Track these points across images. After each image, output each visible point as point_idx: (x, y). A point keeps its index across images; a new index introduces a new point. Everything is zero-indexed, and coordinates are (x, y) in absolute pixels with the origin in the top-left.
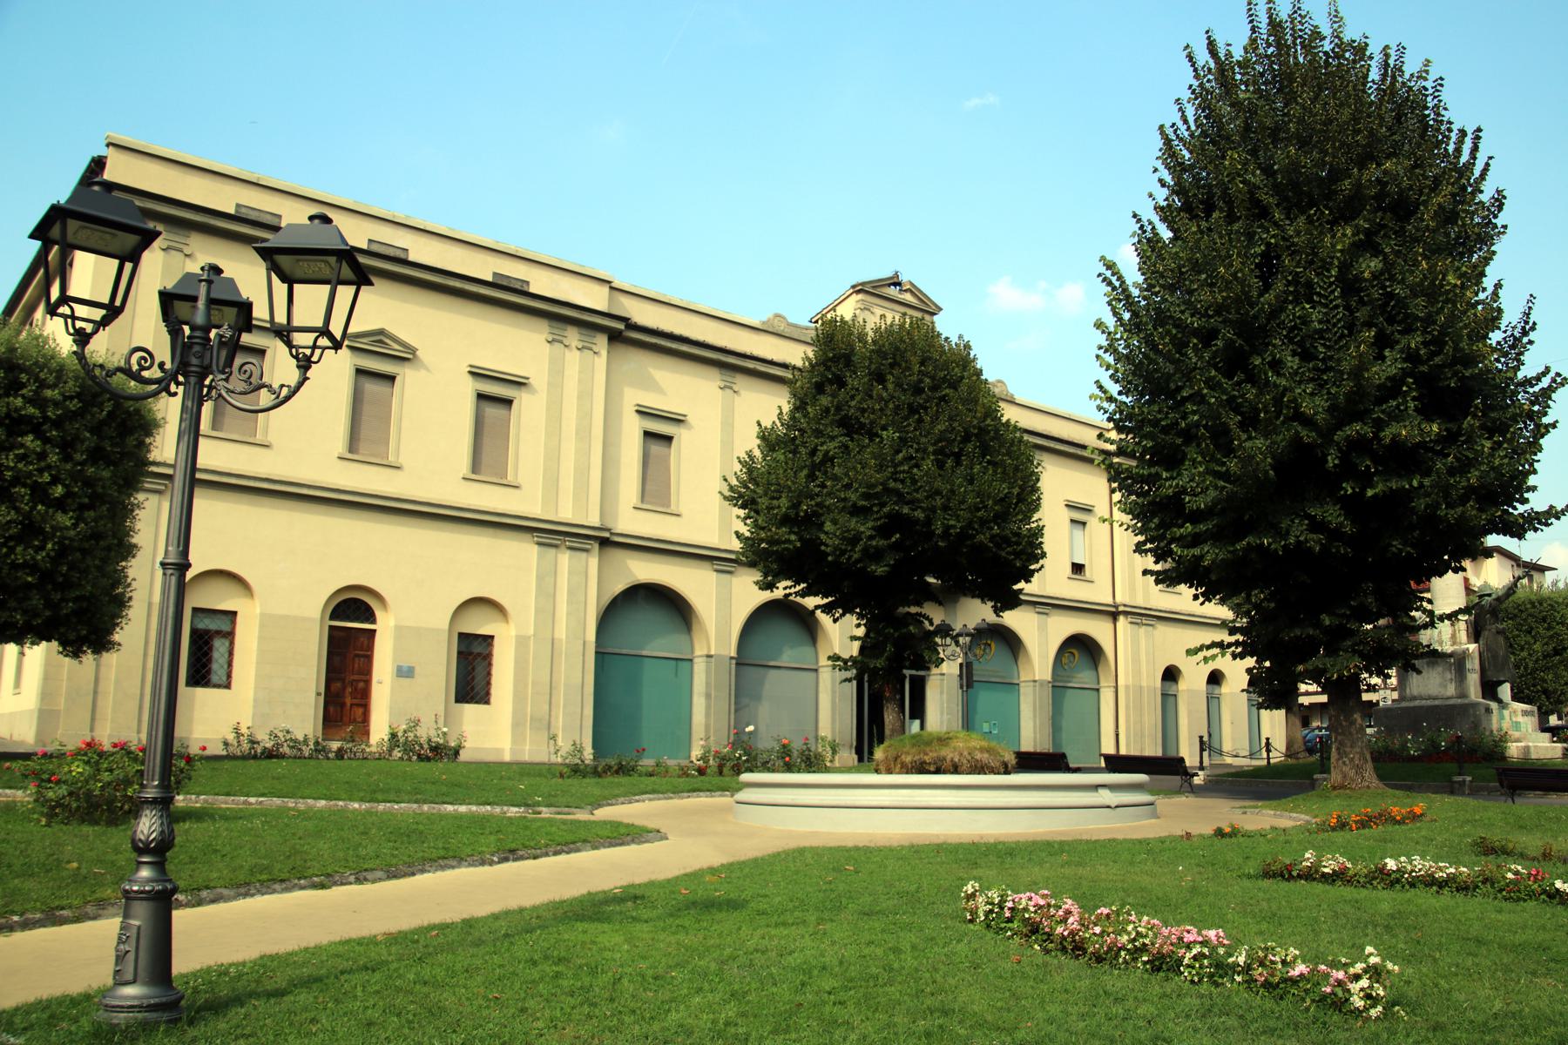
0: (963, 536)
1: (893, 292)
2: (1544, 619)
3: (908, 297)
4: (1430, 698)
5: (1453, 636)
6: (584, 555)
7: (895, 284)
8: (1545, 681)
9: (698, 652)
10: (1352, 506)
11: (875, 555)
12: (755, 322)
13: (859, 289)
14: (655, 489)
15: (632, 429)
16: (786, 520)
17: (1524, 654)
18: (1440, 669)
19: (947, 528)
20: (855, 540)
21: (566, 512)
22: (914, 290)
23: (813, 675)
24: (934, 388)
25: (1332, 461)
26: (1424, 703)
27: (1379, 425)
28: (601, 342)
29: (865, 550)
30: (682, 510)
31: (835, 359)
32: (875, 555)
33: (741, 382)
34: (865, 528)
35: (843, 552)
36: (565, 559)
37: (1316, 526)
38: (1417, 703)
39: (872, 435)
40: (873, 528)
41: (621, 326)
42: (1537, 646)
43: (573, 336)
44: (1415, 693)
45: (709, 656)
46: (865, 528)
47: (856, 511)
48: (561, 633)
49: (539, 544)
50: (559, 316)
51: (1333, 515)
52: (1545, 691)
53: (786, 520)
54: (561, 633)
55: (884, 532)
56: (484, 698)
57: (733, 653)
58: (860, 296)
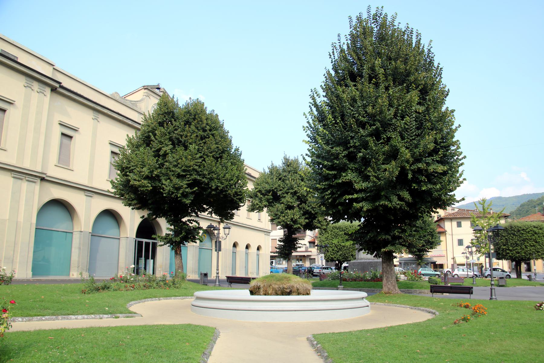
1: (157, 91)
6: (34, 184)
7: (159, 88)
9: (75, 230)
10: (412, 193)
11: (185, 195)
12: (108, 94)
13: (146, 88)
14: (64, 159)
15: (58, 130)
16: (147, 178)
19: (217, 187)
20: (178, 189)
21: (27, 164)
24: (210, 130)
25: (410, 176)
26: (366, 261)
27: (428, 164)
28: (48, 90)
29: (182, 194)
30: (74, 168)
31: (168, 113)
32: (185, 195)
33: (101, 118)
34: (184, 183)
35: (173, 193)
36: (25, 185)
37: (401, 199)
38: (363, 261)
39: (186, 148)
40: (187, 184)
41: (57, 85)
43: (36, 86)
45: (81, 232)
46: (184, 183)
47: (179, 176)
48: (21, 218)
49: (14, 177)
50: (31, 75)
51: (406, 195)
53: (147, 178)
54: (21, 218)
55: (190, 186)
57: (90, 231)
58: (146, 91)
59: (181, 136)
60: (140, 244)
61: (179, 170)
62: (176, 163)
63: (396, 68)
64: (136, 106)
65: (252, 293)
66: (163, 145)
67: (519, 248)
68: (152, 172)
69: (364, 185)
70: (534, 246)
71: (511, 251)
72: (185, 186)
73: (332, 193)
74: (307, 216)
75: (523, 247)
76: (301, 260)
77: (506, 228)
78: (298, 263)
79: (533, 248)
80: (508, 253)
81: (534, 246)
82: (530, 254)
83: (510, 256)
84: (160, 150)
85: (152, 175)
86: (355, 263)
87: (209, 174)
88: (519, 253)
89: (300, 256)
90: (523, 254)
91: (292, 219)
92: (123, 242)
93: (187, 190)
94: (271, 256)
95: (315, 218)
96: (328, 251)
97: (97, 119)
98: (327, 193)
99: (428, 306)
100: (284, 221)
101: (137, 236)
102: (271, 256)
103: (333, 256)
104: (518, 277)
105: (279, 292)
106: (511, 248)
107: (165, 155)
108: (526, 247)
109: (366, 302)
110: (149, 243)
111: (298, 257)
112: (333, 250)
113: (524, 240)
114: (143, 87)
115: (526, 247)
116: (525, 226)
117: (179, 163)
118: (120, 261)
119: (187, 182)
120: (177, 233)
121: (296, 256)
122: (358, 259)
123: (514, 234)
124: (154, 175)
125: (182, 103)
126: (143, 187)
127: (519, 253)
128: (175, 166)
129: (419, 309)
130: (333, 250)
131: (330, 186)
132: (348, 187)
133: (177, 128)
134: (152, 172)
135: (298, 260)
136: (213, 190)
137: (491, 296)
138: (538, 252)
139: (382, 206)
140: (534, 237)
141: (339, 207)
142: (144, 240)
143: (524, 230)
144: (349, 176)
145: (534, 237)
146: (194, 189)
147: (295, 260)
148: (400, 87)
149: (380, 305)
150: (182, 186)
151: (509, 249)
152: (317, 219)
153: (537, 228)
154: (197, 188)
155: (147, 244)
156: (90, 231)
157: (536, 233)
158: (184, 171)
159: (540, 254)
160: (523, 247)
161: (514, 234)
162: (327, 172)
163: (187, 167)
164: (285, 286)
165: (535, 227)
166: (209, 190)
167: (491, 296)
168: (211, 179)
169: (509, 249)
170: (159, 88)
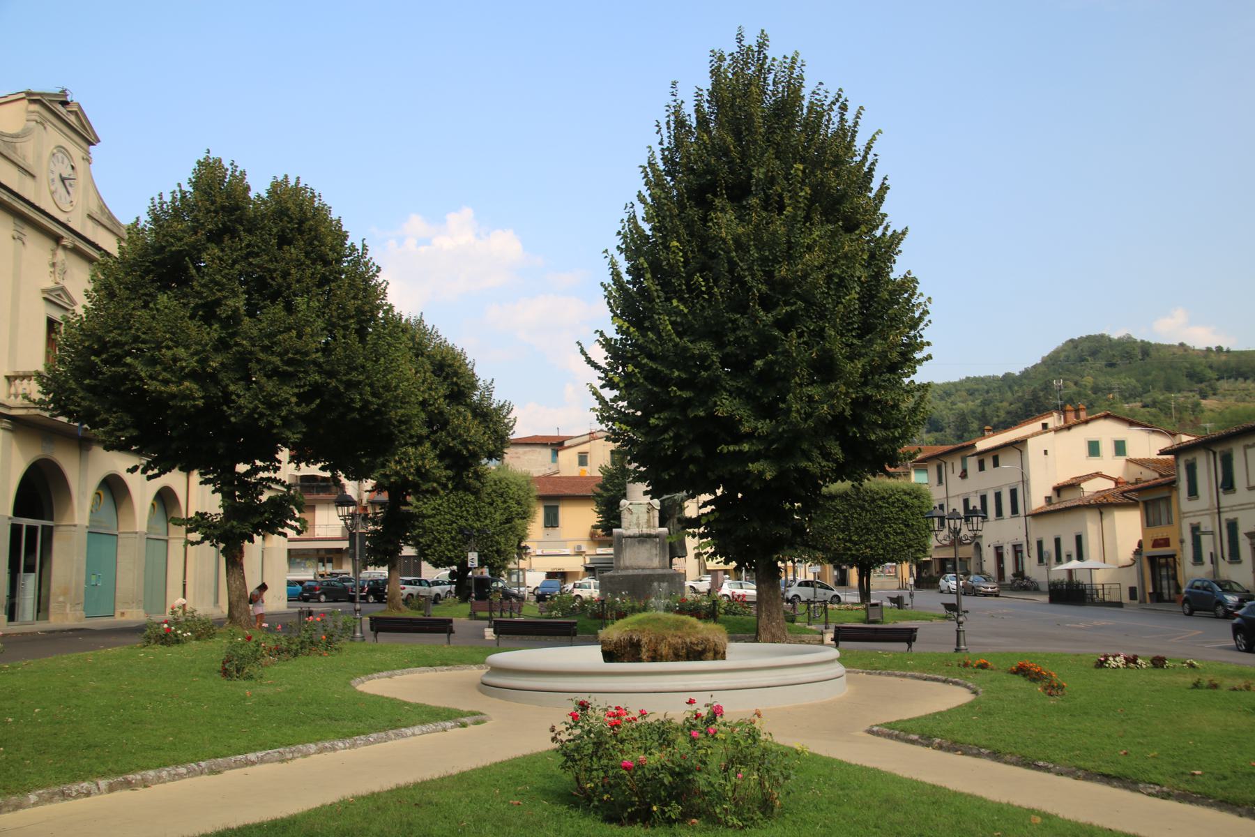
0: (378, 412)
2: (502, 495)
3: (72, 119)
4: (639, 568)
5: (648, 521)
8: (498, 543)
13: (33, 98)
16: (193, 375)
17: (488, 521)
18: (648, 546)
19: (366, 404)
20: (274, 406)
22: (79, 114)
26: (636, 572)
34: (288, 392)
35: (262, 415)
38: (630, 572)
40: (297, 395)
42: (497, 516)
44: (628, 563)
47: (274, 373)
52: (498, 552)
53: (193, 375)
55: (303, 398)
56: (913, 631)
58: (36, 107)
59: (270, 271)
60: (16, 530)
61: (276, 360)
62: (266, 342)
63: (822, 183)
64: (15, 150)
65: (609, 656)
67: (873, 537)
68: (203, 361)
69: (764, 426)
70: (902, 533)
71: (855, 543)
72: (294, 400)
73: (677, 437)
74: (447, 461)
75: (881, 535)
76: (330, 561)
78: (321, 570)
80: (850, 549)
81: (902, 533)
82: (894, 550)
83: (852, 555)
84: (218, 303)
85: (204, 369)
86: (613, 577)
87: (348, 373)
88: (872, 548)
90: (881, 552)
91: (418, 469)
93: (297, 410)
94: (289, 551)
95: (467, 466)
96: (439, 542)
98: (666, 436)
99: (913, 668)
100: (397, 473)
101: (19, 510)
102: (289, 551)
103: (453, 554)
104: (862, 602)
105: (683, 652)
106: (855, 538)
107: (234, 318)
108: (887, 536)
109: (839, 669)
110: (36, 528)
112: (453, 539)
113: (883, 521)
114: (29, 94)
115: (887, 536)
116: (886, 491)
117: (275, 343)
119: (296, 390)
120: (231, 510)
121: (318, 550)
122: (618, 568)
123: (862, 508)
124: (209, 370)
125: (259, 187)
128: (265, 349)
129: (889, 675)
130: (453, 539)
131: (671, 423)
132: (729, 429)
134: (203, 361)
136: (354, 409)
137: (958, 644)
138: (910, 546)
139: (797, 469)
140: (903, 516)
141: (691, 467)
142: (26, 522)
143: (883, 498)
144: (725, 405)
146: (313, 406)
148: (830, 227)
149: (872, 668)
150: (287, 399)
151: (850, 541)
153: (909, 494)
155: (32, 531)
157: (907, 506)
158: (290, 362)
160: (881, 535)
161: (862, 508)
162: (679, 393)
163: (298, 352)
164: (694, 640)
165: (906, 493)
167: (958, 644)
168: (350, 385)
169: (850, 541)
170: (65, 103)
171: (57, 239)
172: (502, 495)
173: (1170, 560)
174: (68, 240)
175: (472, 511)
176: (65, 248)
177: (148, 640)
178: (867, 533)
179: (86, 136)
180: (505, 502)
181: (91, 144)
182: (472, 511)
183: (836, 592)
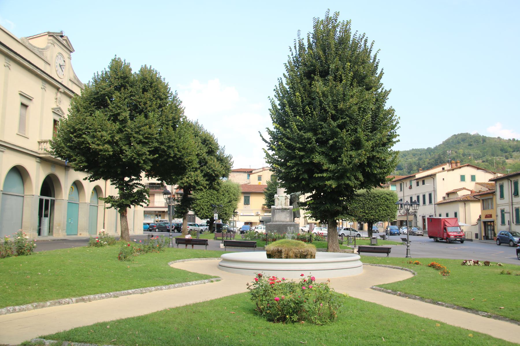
0: (180, 158)
2: (228, 192)
3: (64, 42)
5: (285, 203)
7: (62, 36)
8: (226, 210)
13: (50, 34)
16: (109, 142)
17: (222, 202)
18: (285, 213)
20: (139, 155)
22: (67, 41)
23: (22, 198)
26: (280, 223)
33: (13, 66)
34: (145, 150)
35: (135, 159)
38: (278, 223)
40: (149, 151)
42: (226, 200)
44: (277, 220)
47: (140, 142)
52: (226, 214)
53: (109, 142)
55: (151, 152)
57: (2, 189)
58: (51, 38)
59: (139, 102)
60: (41, 201)
61: (141, 137)
62: (137, 130)
64: (43, 54)
65: (269, 256)
66: (121, 111)
68: (112, 137)
69: (332, 167)
70: (386, 210)
71: (367, 214)
72: (148, 153)
73: (298, 170)
74: (207, 178)
75: (377, 211)
76: (160, 216)
77: (364, 194)
78: (157, 219)
79: (385, 212)
80: (364, 216)
81: (386, 210)
82: (382, 217)
83: (366, 218)
84: (118, 114)
85: (113, 140)
88: (373, 215)
89: (159, 212)
90: (377, 217)
91: (195, 181)
92: (27, 200)
93: (149, 157)
95: (214, 180)
96: (203, 209)
97: (8, 67)
98: (293, 170)
100: (187, 182)
101: (43, 193)
103: (208, 214)
104: (369, 237)
105: (299, 255)
106: (367, 212)
109: (360, 263)
111: (157, 213)
112: (208, 208)
113: (378, 205)
114: (49, 33)
117: (140, 130)
118: (24, 220)
119: (149, 149)
120: (123, 196)
122: (273, 221)
123: (370, 200)
124: (115, 140)
125: (135, 69)
126: (105, 151)
127: (373, 215)
128: (137, 133)
129: (380, 266)
130: (208, 208)
131: (296, 165)
132: (318, 167)
133: (134, 94)
134: (112, 137)
135: (157, 215)
136: (171, 157)
138: (388, 215)
139: (345, 184)
140: (386, 203)
141: (303, 182)
142: (45, 198)
143: (378, 196)
144: (317, 158)
145: (386, 203)
146: (155, 156)
147: (154, 216)
148: (360, 88)
149: (373, 263)
150: (145, 153)
151: (365, 213)
152: (216, 181)
154: (157, 155)
155: (47, 201)
156: (2, 189)
157: (388, 200)
158: (146, 138)
159: (389, 217)
160: (377, 211)
161: (370, 200)
162: (299, 153)
163: (149, 134)
164: (303, 250)
165: (387, 194)
166: (166, 157)
168: (169, 147)
169: (365, 213)
170: (62, 36)
171: (58, 89)
172: (228, 192)
173: (492, 224)
174: (62, 89)
175: (216, 198)
176: (61, 92)
177: (90, 245)
178: (371, 210)
179: (70, 49)
180: (229, 194)
181: (71, 52)
182: (216, 198)
183: (359, 233)
